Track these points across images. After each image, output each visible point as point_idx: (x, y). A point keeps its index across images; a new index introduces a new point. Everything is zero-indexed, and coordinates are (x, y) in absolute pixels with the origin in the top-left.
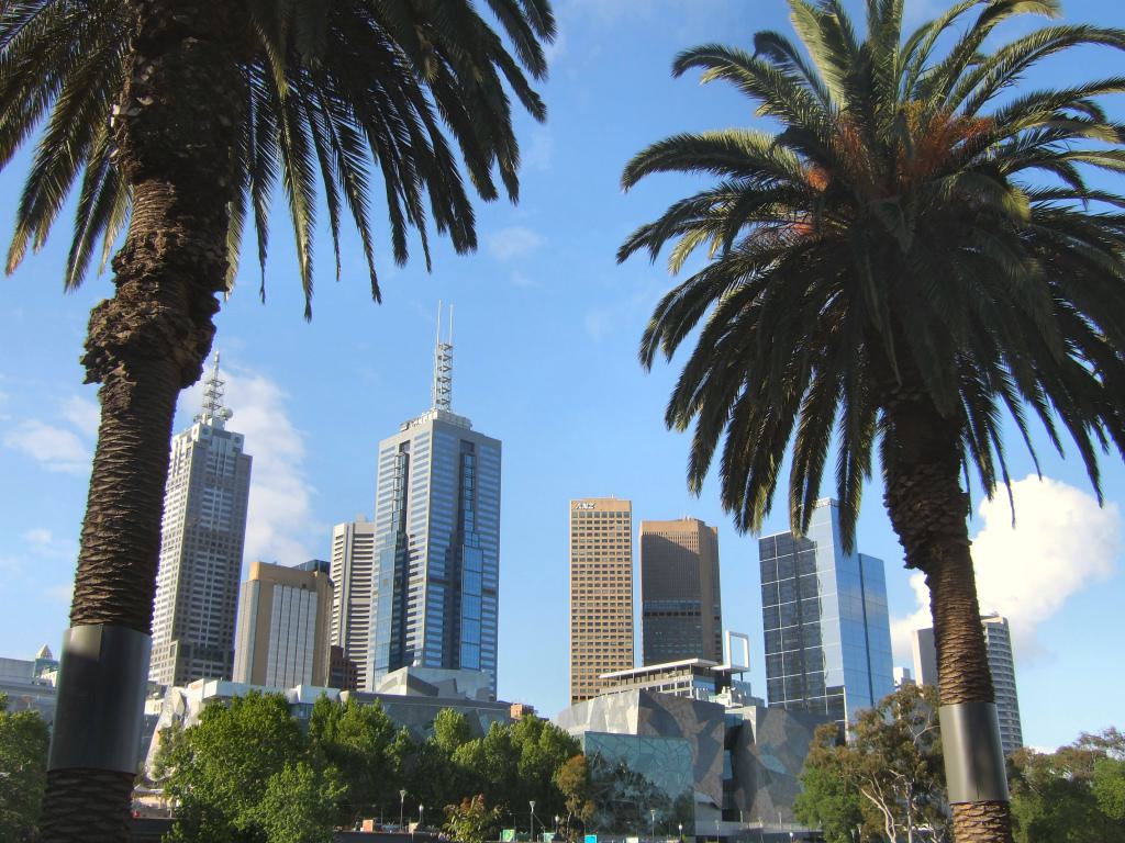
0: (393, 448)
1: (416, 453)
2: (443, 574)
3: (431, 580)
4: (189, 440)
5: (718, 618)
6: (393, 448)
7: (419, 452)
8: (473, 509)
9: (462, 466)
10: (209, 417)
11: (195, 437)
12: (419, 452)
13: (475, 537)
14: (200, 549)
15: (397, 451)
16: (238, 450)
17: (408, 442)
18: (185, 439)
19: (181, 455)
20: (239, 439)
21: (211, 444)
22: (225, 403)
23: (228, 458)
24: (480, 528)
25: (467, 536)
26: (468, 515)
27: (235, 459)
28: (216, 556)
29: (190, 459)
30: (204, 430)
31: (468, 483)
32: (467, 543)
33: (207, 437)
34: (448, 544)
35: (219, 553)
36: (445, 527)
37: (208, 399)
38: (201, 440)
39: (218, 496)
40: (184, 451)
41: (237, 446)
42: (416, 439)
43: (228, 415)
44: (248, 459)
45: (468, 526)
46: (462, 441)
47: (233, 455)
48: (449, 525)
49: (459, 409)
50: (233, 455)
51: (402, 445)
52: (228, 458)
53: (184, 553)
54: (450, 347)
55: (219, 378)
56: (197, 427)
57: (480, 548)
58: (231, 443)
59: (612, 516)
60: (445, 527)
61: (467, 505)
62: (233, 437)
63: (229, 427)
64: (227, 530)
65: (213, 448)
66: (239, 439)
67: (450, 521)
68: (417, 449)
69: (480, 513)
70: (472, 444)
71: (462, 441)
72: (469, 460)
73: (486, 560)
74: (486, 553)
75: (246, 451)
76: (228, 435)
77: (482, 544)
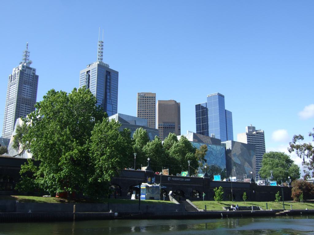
0: (85, 73)
1: (92, 74)
4: (18, 69)
5: (180, 129)
6: (85, 73)
7: (93, 74)
8: (110, 92)
9: (106, 78)
10: (24, 63)
11: (20, 69)
13: (110, 101)
14: (22, 103)
15: (86, 74)
16: (34, 74)
17: (89, 71)
18: (17, 69)
19: (16, 74)
20: (34, 70)
21: (26, 71)
22: (31, 58)
23: (31, 76)
24: (112, 98)
25: (108, 100)
26: (108, 94)
27: (33, 76)
28: (27, 106)
29: (19, 75)
30: (23, 67)
31: (108, 84)
32: (108, 102)
33: (24, 69)
34: (102, 102)
35: (28, 105)
36: (101, 97)
37: (24, 57)
38: (22, 70)
39: (28, 87)
40: (17, 73)
41: (34, 72)
42: (92, 70)
43: (30, 63)
44: (37, 77)
45: (108, 97)
46: (106, 71)
47: (33, 75)
49: (105, 61)
50: (33, 75)
52: (31, 76)
53: (17, 105)
54: (103, 42)
55: (28, 51)
56: (21, 65)
57: (112, 104)
58: (32, 71)
59: (150, 98)
60: (101, 97)
61: (108, 91)
62: (32, 69)
63: (31, 66)
64: (31, 98)
66: (34, 70)
67: (103, 95)
68: (92, 73)
69: (112, 94)
70: (110, 72)
71: (106, 71)
72: (108, 77)
73: (113, 108)
74: (114, 106)
75: (37, 74)
76: (31, 69)
77: (112, 103)
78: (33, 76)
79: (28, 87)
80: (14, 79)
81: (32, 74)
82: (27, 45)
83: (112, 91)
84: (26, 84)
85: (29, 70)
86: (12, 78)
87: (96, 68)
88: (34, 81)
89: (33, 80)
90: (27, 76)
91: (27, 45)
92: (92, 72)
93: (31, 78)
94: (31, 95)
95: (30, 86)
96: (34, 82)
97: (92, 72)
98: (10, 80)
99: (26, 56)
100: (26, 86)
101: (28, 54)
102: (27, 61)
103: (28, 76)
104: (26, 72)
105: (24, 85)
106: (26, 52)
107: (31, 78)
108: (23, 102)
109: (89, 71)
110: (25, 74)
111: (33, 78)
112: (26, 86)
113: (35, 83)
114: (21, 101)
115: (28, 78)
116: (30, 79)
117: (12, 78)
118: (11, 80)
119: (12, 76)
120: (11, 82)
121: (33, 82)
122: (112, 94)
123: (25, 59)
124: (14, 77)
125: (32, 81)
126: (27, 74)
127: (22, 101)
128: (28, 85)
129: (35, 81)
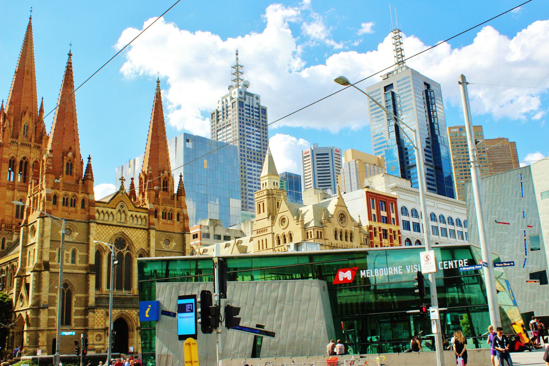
0: (379, 90)
1: (399, 90)
6: (379, 90)
17: (392, 84)
21: (245, 99)
23: (255, 108)
32: (439, 142)
37: (235, 77)
41: (258, 101)
42: (398, 82)
43: (246, 86)
50: (257, 107)
51: (386, 88)
52: (255, 108)
55: (239, 64)
56: (236, 90)
62: (255, 97)
63: (249, 90)
68: (378, 92)
78: (258, 109)
80: (224, 117)
81: (255, 105)
82: (237, 54)
84: (249, 125)
85: (251, 98)
86: (218, 116)
88: (261, 117)
89: (258, 117)
90: (249, 110)
91: (237, 54)
92: (398, 86)
95: (256, 127)
96: (261, 119)
98: (215, 119)
99: (238, 72)
101: (240, 70)
102: (241, 83)
103: (251, 109)
104: (246, 102)
106: (237, 65)
108: (249, 158)
109: (392, 84)
110: (246, 105)
111: (258, 113)
114: (246, 156)
115: (251, 113)
116: (255, 114)
117: (218, 116)
118: (218, 120)
120: (217, 123)
123: (238, 79)
124: (224, 113)
125: (258, 118)
126: (249, 106)
127: (248, 156)
129: (262, 117)
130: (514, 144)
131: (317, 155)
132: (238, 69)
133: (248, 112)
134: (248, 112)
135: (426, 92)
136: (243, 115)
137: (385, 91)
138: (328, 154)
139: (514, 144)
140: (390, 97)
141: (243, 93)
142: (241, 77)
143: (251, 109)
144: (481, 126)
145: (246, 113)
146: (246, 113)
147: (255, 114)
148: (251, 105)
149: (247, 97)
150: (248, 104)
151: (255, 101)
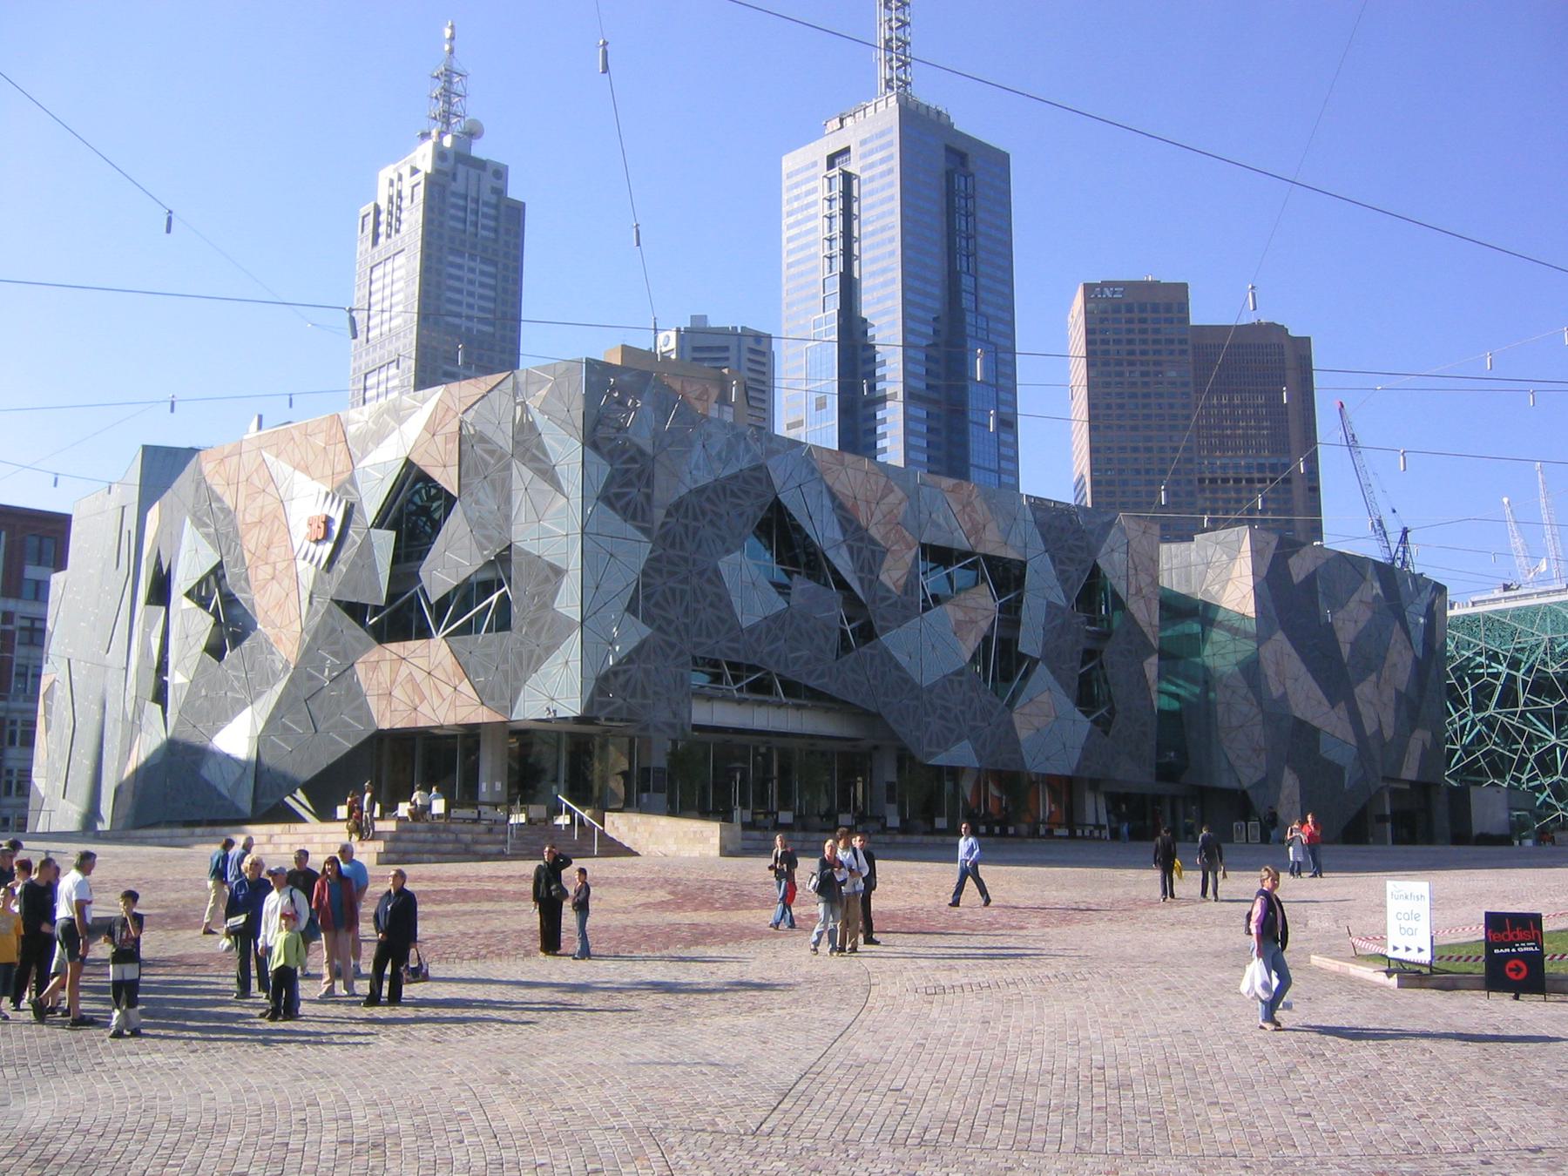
0: (815, 164)
2: (922, 386)
3: (910, 396)
6: (815, 164)
9: (950, 193)
10: (441, 135)
12: (808, 193)
16: (500, 192)
17: (847, 150)
21: (454, 178)
22: (473, 108)
23: (486, 204)
25: (970, 318)
26: (967, 282)
27: (496, 207)
30: (440, 154)
32: (970, 330)
33: (447, 166)
37: (440, 106)
39: (472, 270)
41: (498, 184)
42: (863, 143)
43: (472, 133)
44: (516, 212)
45: (967, 301)
47: (493, 199)
48: (935, 303)
49: (927, 94)
50: (493, 199)
55: (456, 67)
59: (1155, 308)
61: (961, 264)
62: (490, 171)
63: (479, 150)
65: (458, 186)
66: (500, 173)
72: (960, 183)
75: (514, 192)
76: (481, 165)
77: (992, 338)
78: (496, 207)
79: (472, 270)
81: (487, 196)
83: (982, 268)
84: (461, 254)
85: (473, 172)
87: (890, 130)
89: (496, 231)
92: (863, 156)
93: (485, 216)
94: (493, 312)
95: (484, 261)
97: (863, 156)
99: (447, 94)
100: (459, 260)
102: (458, 125)
103: (471, 206)
104: (458, 186)
105: (451, 258)
106: (449, 74)
107: (485, 216)
110: (454, 194)
111: (496, 219)
112: (459, 260)
113: (507, 244)
115: (471, 218)
116: (482, 221)
117: (377, 224)
119: (377, 211)
121: (496, 240)
122: (982, 281)
128: (472, 257)
129: (507, 232)
130: (1305, 342)
131: (695, 349)
132: (449, 83)
133: (461, 214)
134: (461, 214)
135: (949, 176)
136: (441, 225)
137: (831, 165)
138: (726, 349)
139: (1305, 342)
140: (838, 184)
141: (451, 161)
142: (457, 109)
143: (471, 206)
144: (1185, 286)
145: (453, 218)
146: (453, 218)
147: (482, 221)
148: (473, 193)
149: (462, 170)
150: (462, 191)
151: (488, 182)
